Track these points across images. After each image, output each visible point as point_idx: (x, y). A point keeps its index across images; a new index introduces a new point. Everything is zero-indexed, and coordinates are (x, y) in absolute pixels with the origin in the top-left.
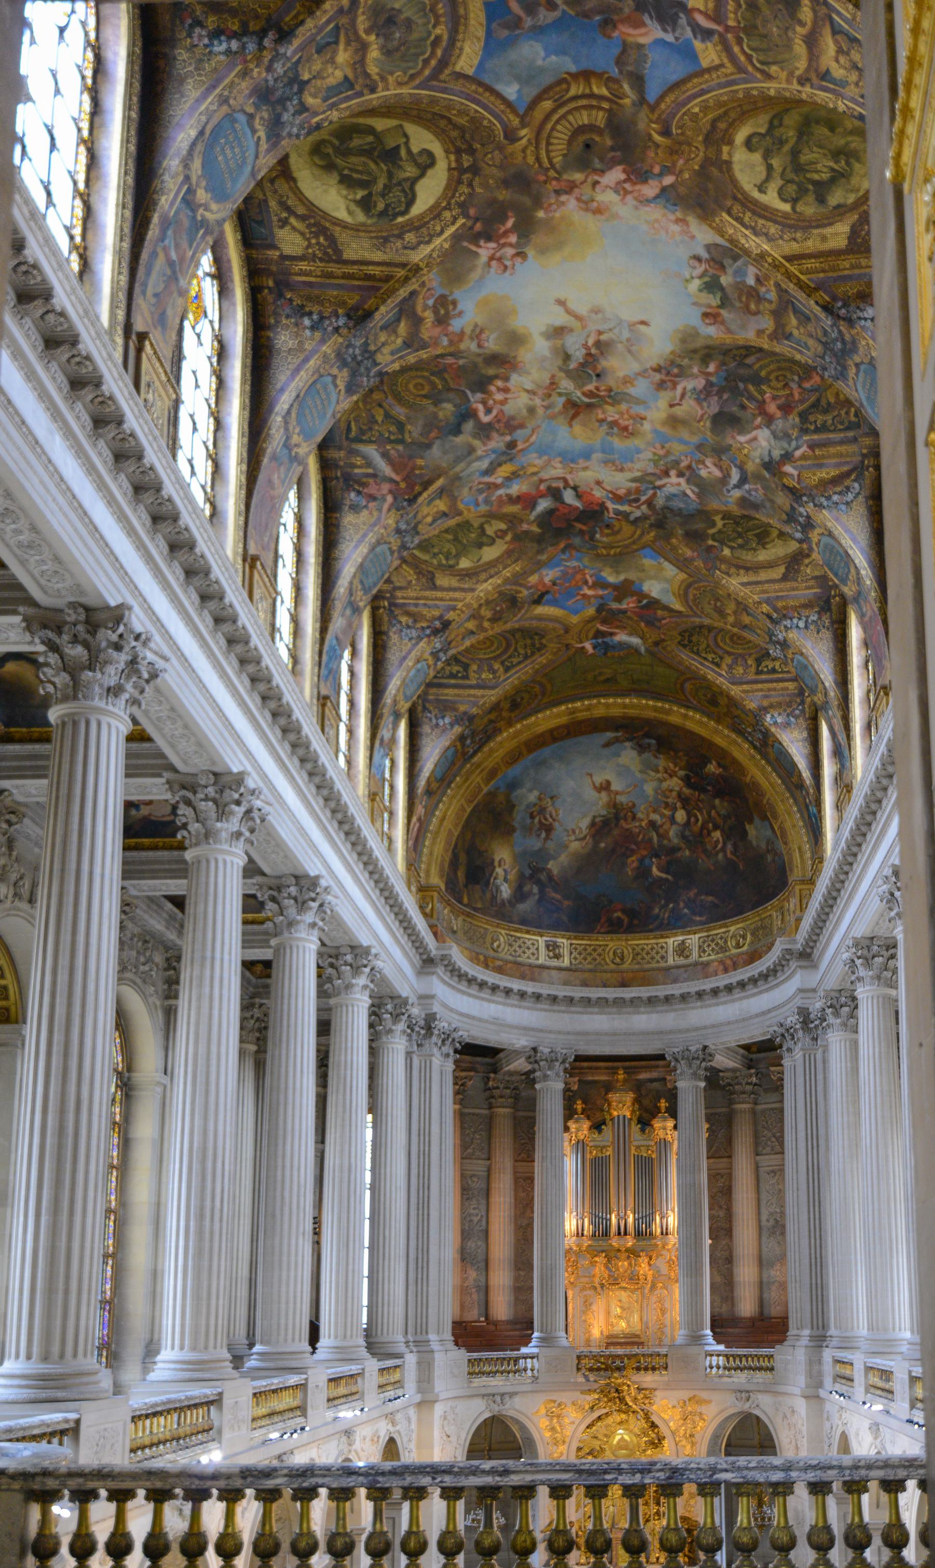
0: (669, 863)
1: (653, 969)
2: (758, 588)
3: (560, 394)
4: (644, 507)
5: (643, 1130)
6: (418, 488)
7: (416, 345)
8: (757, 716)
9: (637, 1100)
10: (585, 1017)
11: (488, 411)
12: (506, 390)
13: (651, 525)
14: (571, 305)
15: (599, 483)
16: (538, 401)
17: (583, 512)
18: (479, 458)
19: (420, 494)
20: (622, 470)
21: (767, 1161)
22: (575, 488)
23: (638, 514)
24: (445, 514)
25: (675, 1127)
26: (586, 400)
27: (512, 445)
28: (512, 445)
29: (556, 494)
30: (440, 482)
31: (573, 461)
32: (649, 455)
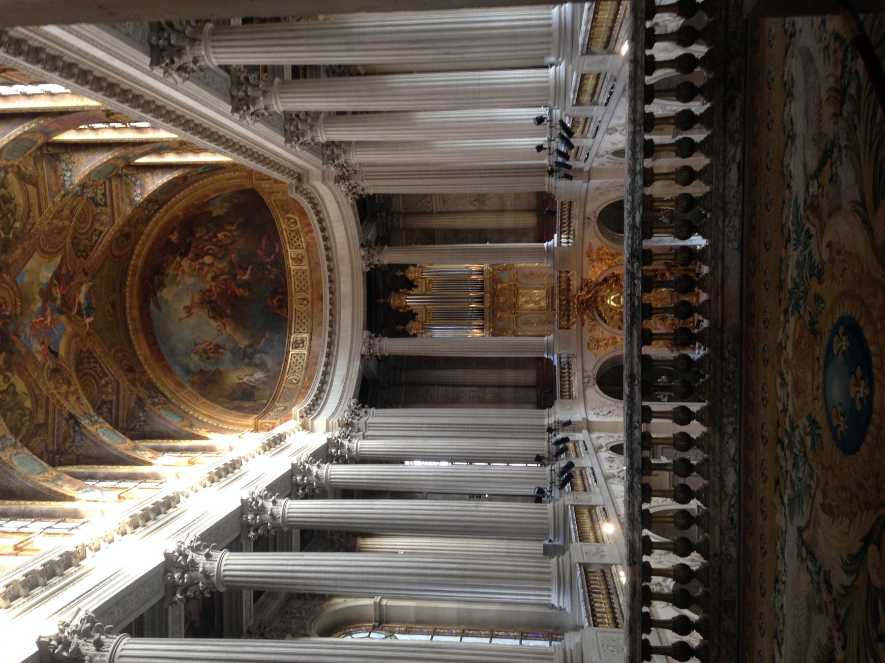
0: (240, 268)
1: (311, 279)
5: (416, 287)
8: (142, 206)
9: (397, 291)
10: (342, 323)
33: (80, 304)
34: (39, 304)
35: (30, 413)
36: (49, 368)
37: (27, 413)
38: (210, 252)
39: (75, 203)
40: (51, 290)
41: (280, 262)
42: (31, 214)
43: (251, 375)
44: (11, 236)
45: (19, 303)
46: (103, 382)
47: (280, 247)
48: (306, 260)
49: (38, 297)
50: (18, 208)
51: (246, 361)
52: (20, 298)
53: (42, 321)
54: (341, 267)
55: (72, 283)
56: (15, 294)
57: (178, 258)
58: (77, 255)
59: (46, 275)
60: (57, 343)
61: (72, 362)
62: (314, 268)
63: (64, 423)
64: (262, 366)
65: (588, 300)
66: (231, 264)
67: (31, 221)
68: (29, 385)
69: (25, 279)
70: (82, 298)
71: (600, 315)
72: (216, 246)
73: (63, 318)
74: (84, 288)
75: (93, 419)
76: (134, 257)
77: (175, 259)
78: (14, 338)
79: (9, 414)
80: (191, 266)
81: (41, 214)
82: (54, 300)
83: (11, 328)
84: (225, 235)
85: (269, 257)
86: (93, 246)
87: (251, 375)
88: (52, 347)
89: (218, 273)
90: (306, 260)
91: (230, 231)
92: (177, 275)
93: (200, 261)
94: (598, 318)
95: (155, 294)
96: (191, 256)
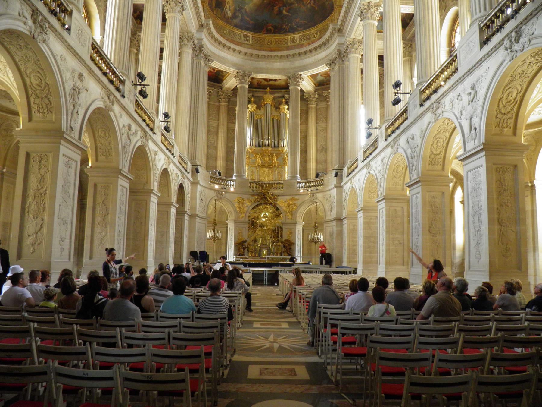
10: (257, 63)
21: (321, 125)
25: (288, 109)
41: (293, 30)
43: (229, 9)
47: (301, 30)
48: (293, 44)
51: (238, 8)
54: (289, 63)
62: (288, 48)
64: (234, 16)
65: (266, 198)
71: (257, 206)
85: (296, 25)
87: (229, 9)
90: (293, 44)
91: (310, 3)
94: (256, 204)
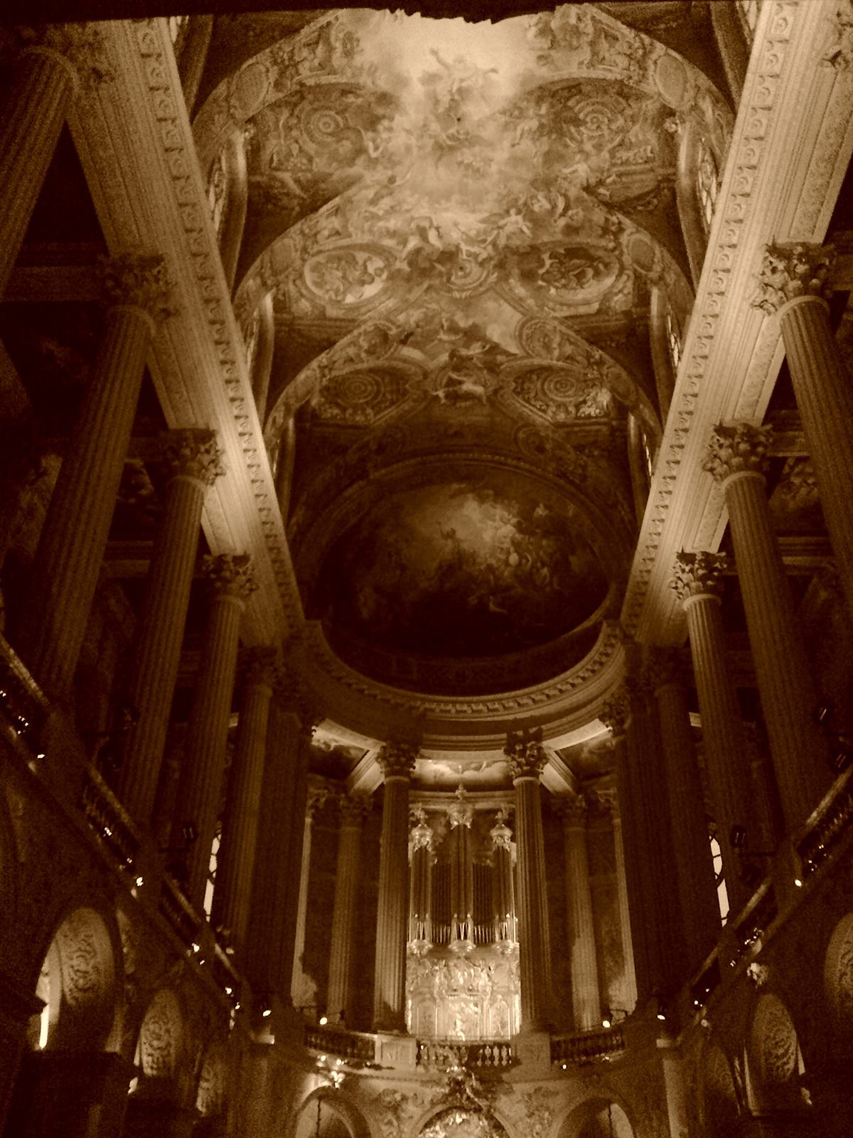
2: (578, 321)
3: (431, 136)
4: (490, 248)
6: (319, 204)
7: (328, 70)
11: (376, 148)
12: (390, 129)
13: (495, 266)
14: (441, 54)
15: (456, 224)
16: (413, 141)
17: (443, 252)
18: (367, 187)
19: (321, 206)
20: (473, 211)
22: (437, 229)
23: (484, 255)
24: (338, 233)
26: (449, 143)
27: (392, 180)
28: (392, 180)
29: (422, 233)
30: (337, 201)
31: (438, 202)
32: (493, 196)
33: (460, 383)
34: (463, 323)
35: (338, 302)
36: (390, 329)
37: (339, 298)
38: (524, 561)
39: (579, 358)
40: (478, 341)
42: (565, 308)
44: (540, 283)
45: (464, 295)
46: (369, 411)
49: (470, 322)
50: (572, 292)
52: (471, 297)
53: (442, 326)
55: (485, 372)
56: (475, 289)
57: (514, 520)
58: (519, 377)
59: (495, 333)
60: (416, 345)
61: (395, 363)
63: (325, 336)
66: (508, 588)
67: (558, 306)
68: (370, 300)
69: (491, 305)
70: (469, 386)
72: (533, 567)
73: (444, 358)
74: (479, 390)
75: (326, 371)
76: (514, 462)
77: (514, 516)
78: (425, 285)
79: (340, 274)
80: (505, 537)
81: (566, 318)
82: (467, 346)
83: (436, 282)
84: (545, 577)
86: (528, 401)
88: (411, 339)
89: (497, 573)
91: (551, 583)
92: (494, 520)
93: (512, 549)
95: (472, 491)
96: (518, 537)
